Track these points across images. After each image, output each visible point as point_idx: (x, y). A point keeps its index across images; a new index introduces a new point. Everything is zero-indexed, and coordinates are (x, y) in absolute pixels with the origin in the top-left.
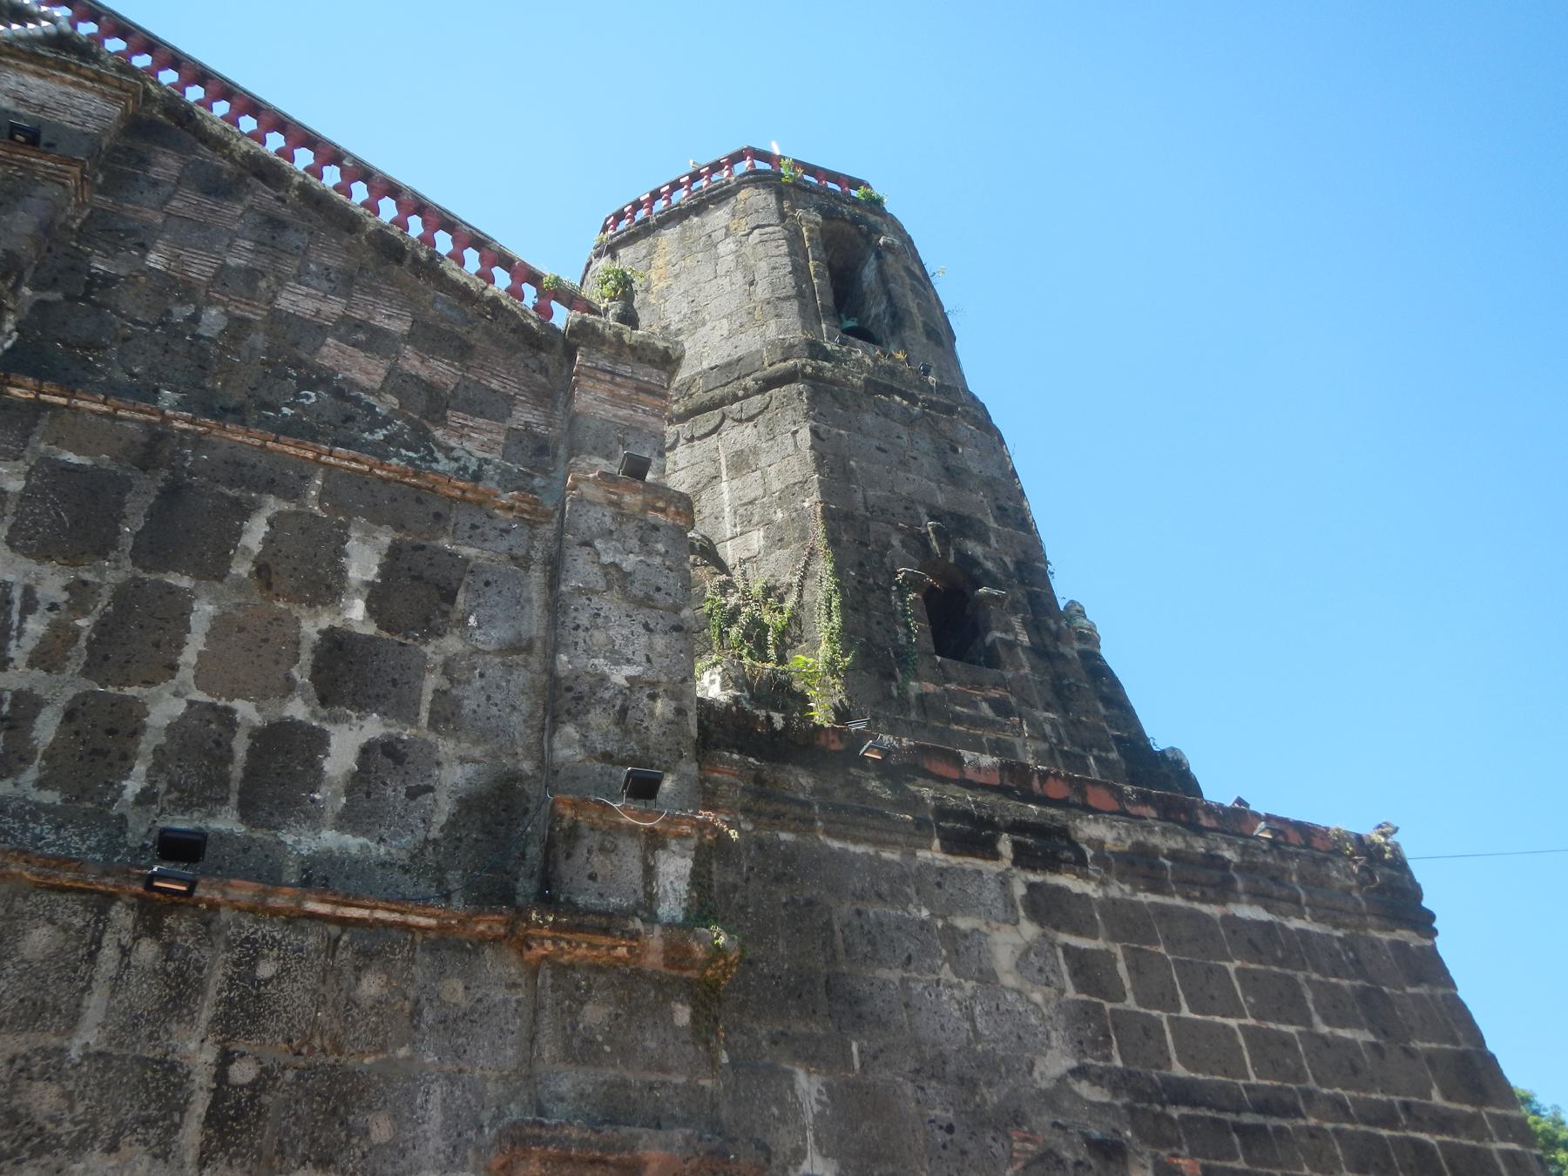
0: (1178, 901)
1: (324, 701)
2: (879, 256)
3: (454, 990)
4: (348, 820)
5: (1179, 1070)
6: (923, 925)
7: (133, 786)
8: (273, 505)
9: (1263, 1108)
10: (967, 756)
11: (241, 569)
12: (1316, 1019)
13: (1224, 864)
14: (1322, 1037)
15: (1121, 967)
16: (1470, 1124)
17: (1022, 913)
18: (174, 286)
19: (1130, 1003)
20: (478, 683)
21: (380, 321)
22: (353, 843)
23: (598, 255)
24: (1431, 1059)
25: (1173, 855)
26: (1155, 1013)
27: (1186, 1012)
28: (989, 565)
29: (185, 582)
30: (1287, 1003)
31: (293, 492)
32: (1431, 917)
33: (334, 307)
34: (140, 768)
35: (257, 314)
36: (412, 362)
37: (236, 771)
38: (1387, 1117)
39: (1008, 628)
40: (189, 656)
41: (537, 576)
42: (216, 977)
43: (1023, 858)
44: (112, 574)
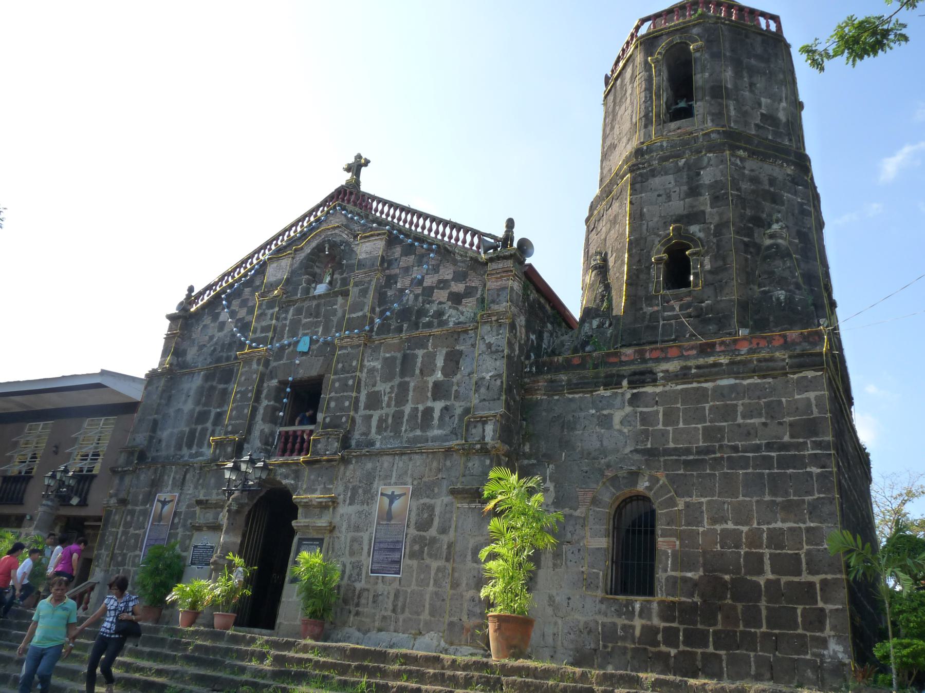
0: (695, 385)
7: (403, 429)
11: (417, 372)
12: (739, 417)
15: (661, 416)
16: (800, 446)
17: (627, 404)
19: (660, 427)
20: (464, 385)
24: (791, 425)
26: (668, 428)
37: (419, 421)
40: (410, 397)
44: (397, 380)
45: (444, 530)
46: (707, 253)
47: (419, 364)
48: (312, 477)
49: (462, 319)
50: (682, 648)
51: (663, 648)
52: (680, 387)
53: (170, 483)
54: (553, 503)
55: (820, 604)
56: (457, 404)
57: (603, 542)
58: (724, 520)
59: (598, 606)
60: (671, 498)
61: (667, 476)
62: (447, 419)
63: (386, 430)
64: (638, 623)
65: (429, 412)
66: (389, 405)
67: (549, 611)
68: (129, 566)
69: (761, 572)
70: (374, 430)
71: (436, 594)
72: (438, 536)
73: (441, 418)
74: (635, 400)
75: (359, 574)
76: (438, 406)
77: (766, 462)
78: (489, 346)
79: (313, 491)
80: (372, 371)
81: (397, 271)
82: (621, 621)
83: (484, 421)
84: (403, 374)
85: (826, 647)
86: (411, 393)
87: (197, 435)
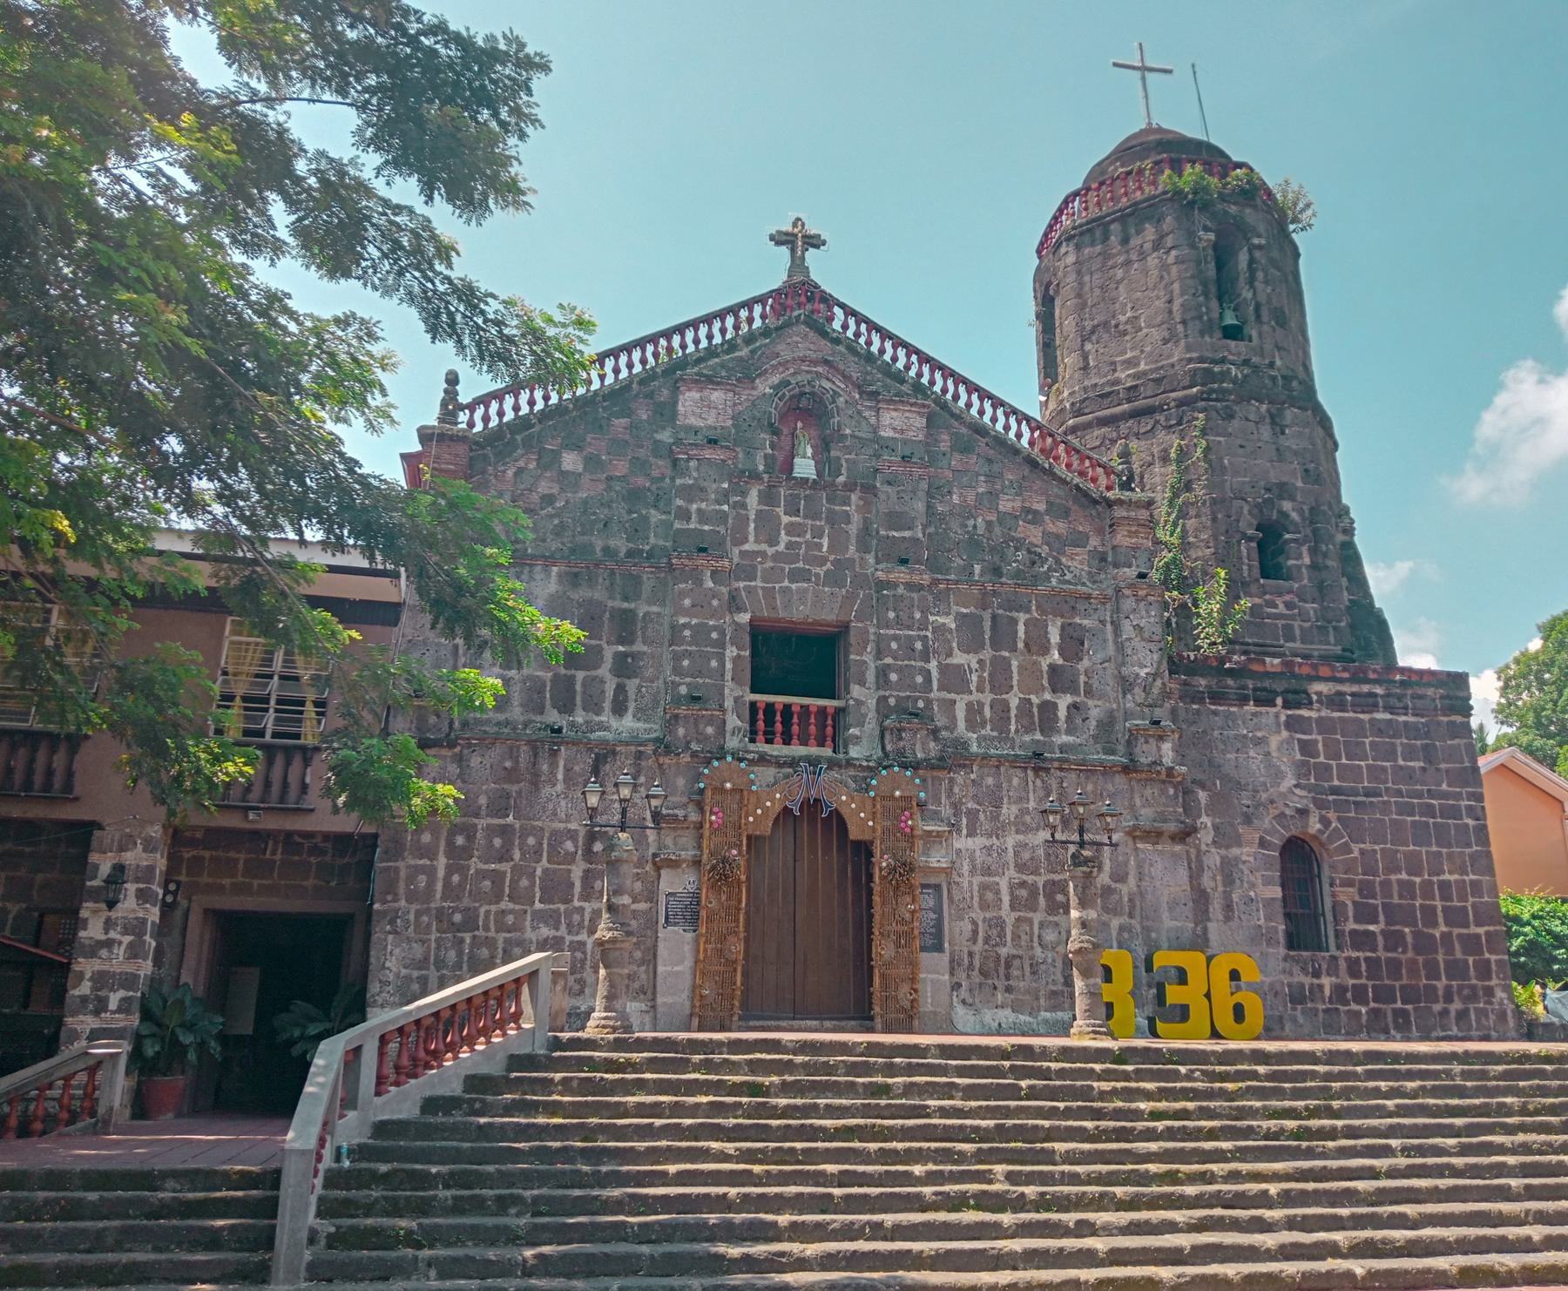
0: (1351, 715)
1: (1054, 691)
2: (1250, 251)
3: (1110, 787)
4: (1069, 732)
5: (1336, 783)
6: (1245, 736)
7: (1013, 728)
8: (1022, 617)
10: (1268, 660)
11: (1021, 645)
13: (1375, 695)
14: (1401, 768)
15: (1320, 746)
16: (1458, 796)
18: (967, 513)
19: (1322, 759)
21: (1036, 506)
22: (1071, 739)
23: (1068, 239)
24: (1447, 771)
25: (1353, 695)
27: (1344, 761)
28: (1294, 515)
29: (1006, 654)
30: (1390, 754)
31: (1028, 611)
32: (1471, 708)
33: (1018, 504)
35: (993, 518)
36: (1051, 528)
38: (1419, 795)
39: (1300, 557)
40: (1015, 682)
41: (1109, 627)
42: (1055, 786)
43: (1286, 706)
45: (1120, 877)
46: (1305, 542)
49: (1068, 577)
50: (1372, 1005)
51: (1354, 1007)
52: (1336, 714)
53: (560, 776)
54: (1214, 842)
55: (1487, 955)
56: (1090, 703)
57: (1277, 892)
58: (1398, 870)
59: (1282, 965)
60: (1346, 843)
61: (1339, 819)
62: (1079, 721)
63: (983, 724)
64: (1327, 982)
65: (1048, 708)
66: (980, 689)
68: (487, 929)
69: (1435, 924)
70: (961, 724)
72: (1113, 885)
73: (1069, 718)
74: (1293, 724)
75: (1002, 935)
76: (1063, 702)
77: (1429, 811)
80: (940, 630)
82: (1307, 980)
87: (578, 688)
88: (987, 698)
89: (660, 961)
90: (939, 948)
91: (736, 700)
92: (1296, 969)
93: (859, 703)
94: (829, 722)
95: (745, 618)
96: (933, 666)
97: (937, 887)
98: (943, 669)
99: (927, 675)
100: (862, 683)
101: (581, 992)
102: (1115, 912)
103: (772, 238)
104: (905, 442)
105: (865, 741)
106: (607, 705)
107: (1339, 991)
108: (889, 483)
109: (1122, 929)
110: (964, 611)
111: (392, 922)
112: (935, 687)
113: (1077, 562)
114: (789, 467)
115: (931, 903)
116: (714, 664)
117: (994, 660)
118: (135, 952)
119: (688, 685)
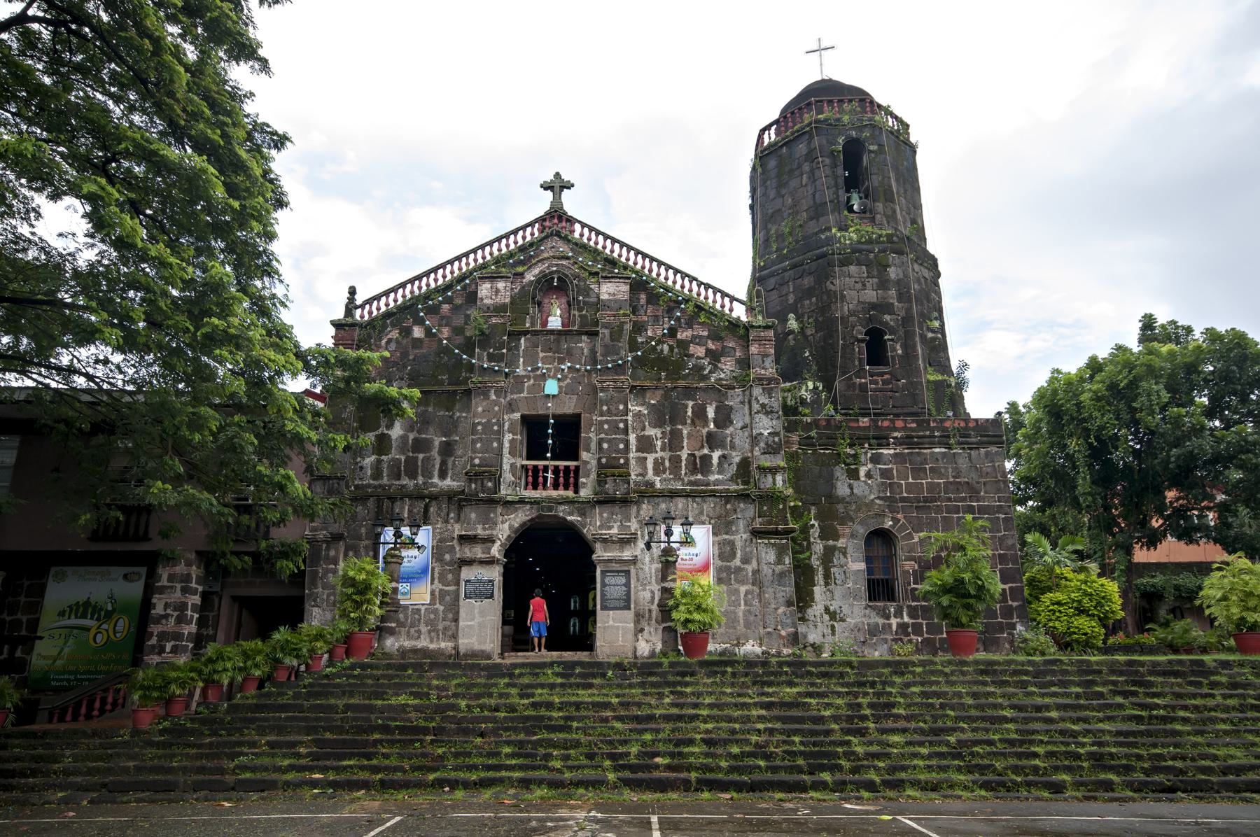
4: (719, 473)
5: (905, 495)
7: (683, 472)
8: (691, 403)
9: (925, 501)
10: (861, 419)
11: (689, 421)
15: (895, 472)
21: (701, 333)
22: (720, 477)
27: (911, 480)
29: (680, 427)
34: (684, 468)
36: (711, 345)
39: (894, 350)
40: (685, 444)
41: (747, 407)
45: (746, 561)
47: (689, 413)
48: (605, 515)
55: (1010, 603)
56: (734, 454)
57: (862, 566)
61: (905, 517)
64: (894, 622)
65: (706, 459)
66: (663, 449)
67: (826, 617)
70: (650, 472)
71: (749, 611)
73: (720, 464)
74: (876, 459)
78: (763, 406)
79: (610, 528)
80: (638, 415)
81: (645, 318)
82: (881, 621)
83: (773, 471)
84: (673, 421)
85: (1015, 629)
86: (685, 441)
87: (419, 464)
88: (666, 455)
89: (461, 620)
90: (628, 608)
91: (512, 465)
92: (873, 614)
93: (586, 463)
94: (572, 475)
95: (517, 416)
96: (632, 438)
97: (628, 573)
98: (639, 439)
99: (627, 443)
100: (588, 450)
101: (419, 637)
102: (742, 582)
103: (542, 187)
104: (616, 301)
105: (589, 484)
106: (436, 473)
107: (903, 627)
108: (606, 328)
109: (747, 593)
110: (653, 402)
111: (315, 600)
112: (633, 447)
113: (728, 366)
114: (545, 323)
115: (624, 581)
116: (495, 445)
117: (672, 432)
118: (181, 620)
119: (480, 458)
